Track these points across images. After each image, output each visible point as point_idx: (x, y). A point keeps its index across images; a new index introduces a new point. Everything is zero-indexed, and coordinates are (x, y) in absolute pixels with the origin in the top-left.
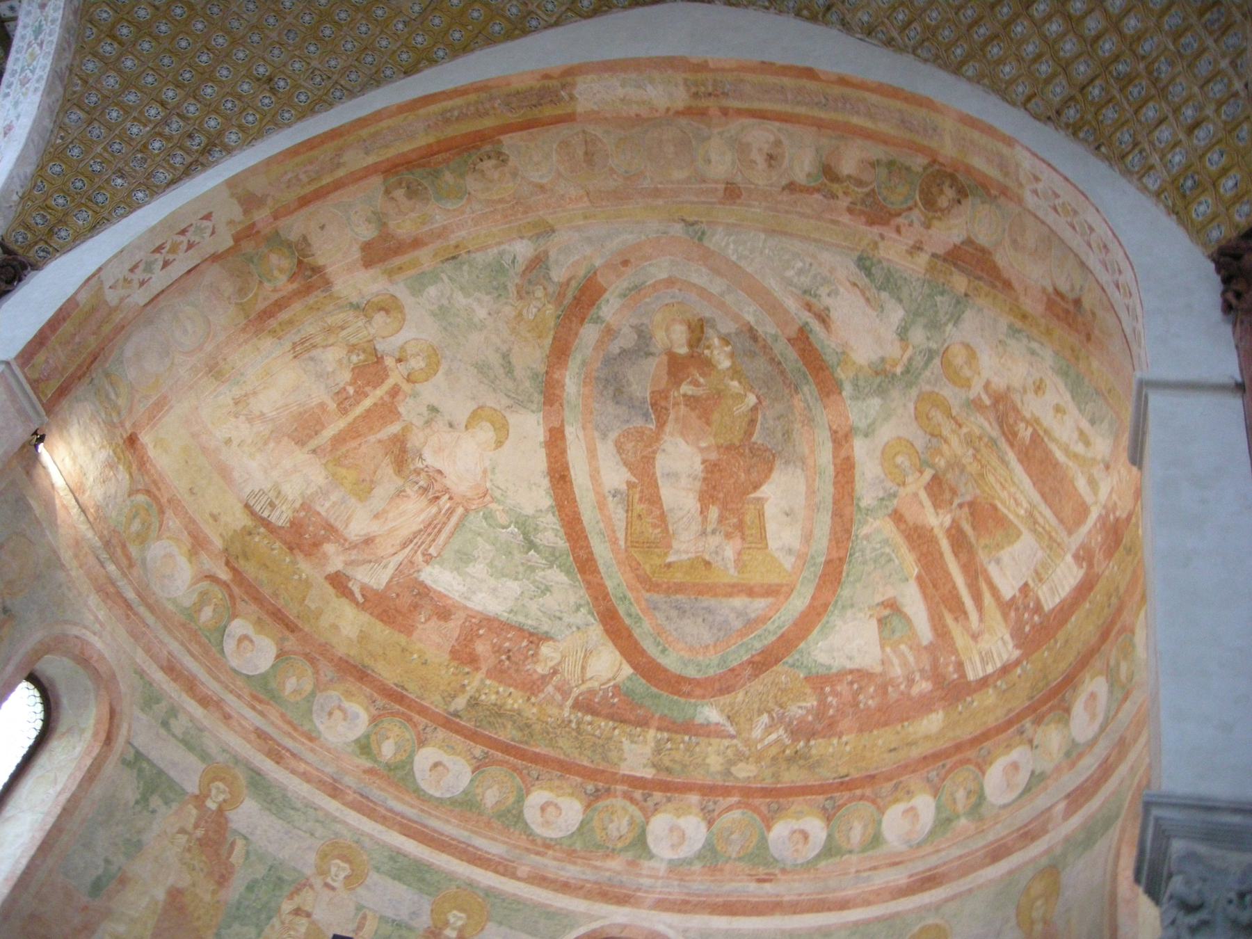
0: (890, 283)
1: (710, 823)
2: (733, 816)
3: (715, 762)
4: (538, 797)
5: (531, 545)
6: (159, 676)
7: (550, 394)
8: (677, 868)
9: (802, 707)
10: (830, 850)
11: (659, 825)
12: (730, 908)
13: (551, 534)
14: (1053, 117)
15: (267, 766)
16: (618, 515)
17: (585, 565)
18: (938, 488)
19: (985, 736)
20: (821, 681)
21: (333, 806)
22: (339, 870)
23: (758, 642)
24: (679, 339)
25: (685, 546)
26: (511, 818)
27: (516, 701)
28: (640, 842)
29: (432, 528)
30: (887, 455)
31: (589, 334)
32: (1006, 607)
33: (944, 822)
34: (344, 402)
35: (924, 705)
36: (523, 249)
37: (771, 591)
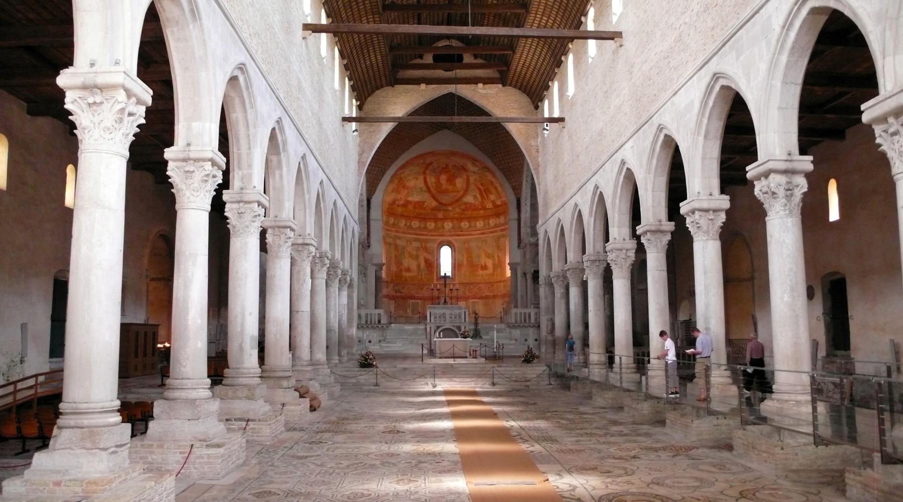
0: (476, 166)
1: (452, 222)
2: (455, 222)
3: (452, 215)
4: (428, 224)
5: (422, 190)
6: (388, 232)
7: (424, 173)
8: (449, 231)
9: (463, 207)
10: (470, 227)
11: (445, 224)
12: (458, 235)
13: (425, 188)
14: (500, 170)
15: (397, 234)
16: (434, 185)
17: (429, 190)
18: (482, 184)
19: (489, 216)
20: (466, 204)
21: (405, 235)
22: (409, 243)
23: (457, 198)
24: (444, 166)
25: (444, 187)
26: (426, 228)
27: (422, 211)
28: (443, 227)
29: (408, 193)
30: (475, 179)
31: (431, 167)
32: (492, 201)
33: (485, 225)
34: (397, 185)
35: (480, 209)
36: (422, 161)
37: (457, 192)
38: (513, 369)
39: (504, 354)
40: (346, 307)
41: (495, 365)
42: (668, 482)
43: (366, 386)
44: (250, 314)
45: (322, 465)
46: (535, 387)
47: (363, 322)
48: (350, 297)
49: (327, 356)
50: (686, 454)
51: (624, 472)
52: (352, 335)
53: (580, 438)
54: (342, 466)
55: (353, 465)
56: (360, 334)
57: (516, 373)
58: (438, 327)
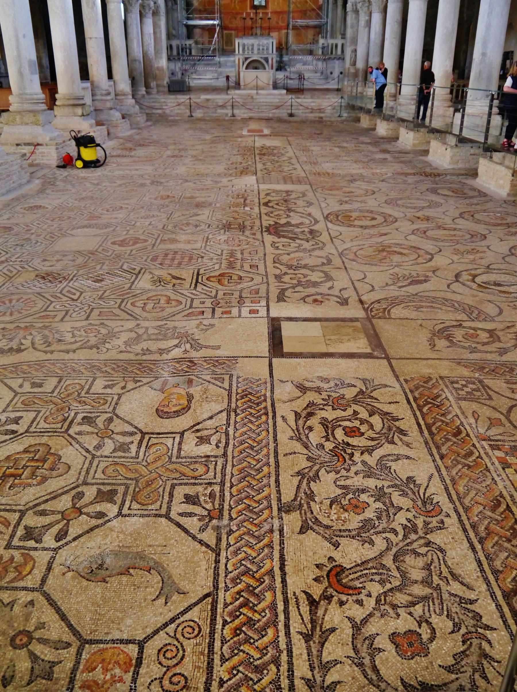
38: (310, 100)
39: (305, 87)
40: (152, 36)
41: (293, 97)
42: (399, 202)
43: (171, 116)
44: (24, 36)
45: (98, 184)
46: (328, 119)
47: (175, 52)
48: (155, 26)
49: (132, 87)
50: (432, 179)
51: (365, 192)
52: (163, 67)
53: (345, 164)
54: (115, 185)
55: (125, 184)
56: (172, 65)
57: (313, 104)
58: (246, 59)
